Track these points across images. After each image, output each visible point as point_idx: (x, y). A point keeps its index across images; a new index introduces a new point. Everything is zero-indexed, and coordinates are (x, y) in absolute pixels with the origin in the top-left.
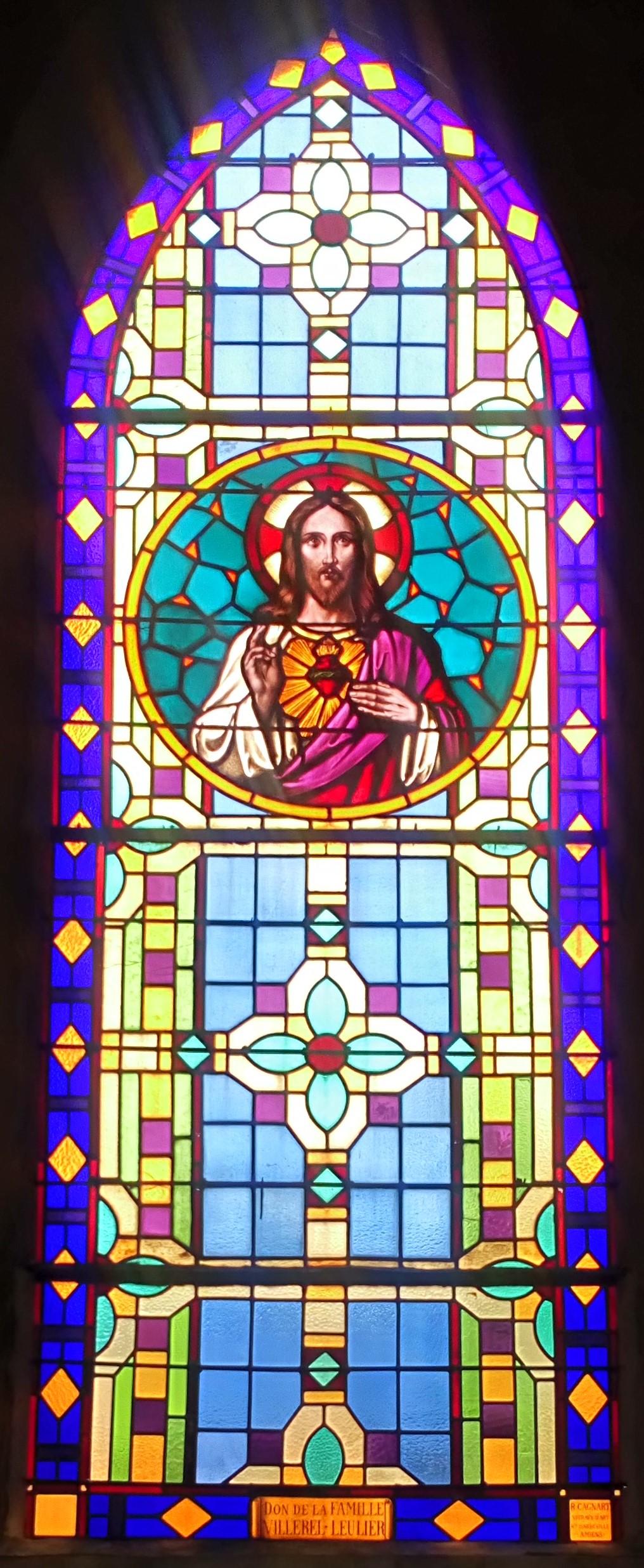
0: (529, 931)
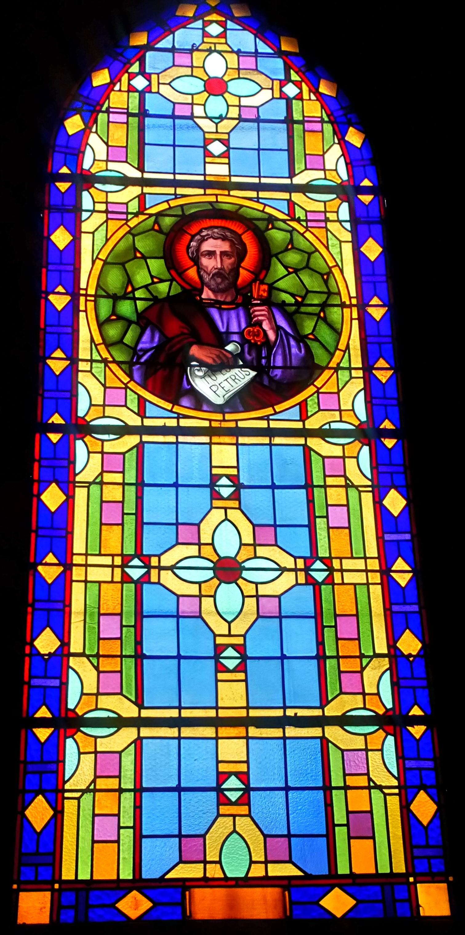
0: (360, 492)
